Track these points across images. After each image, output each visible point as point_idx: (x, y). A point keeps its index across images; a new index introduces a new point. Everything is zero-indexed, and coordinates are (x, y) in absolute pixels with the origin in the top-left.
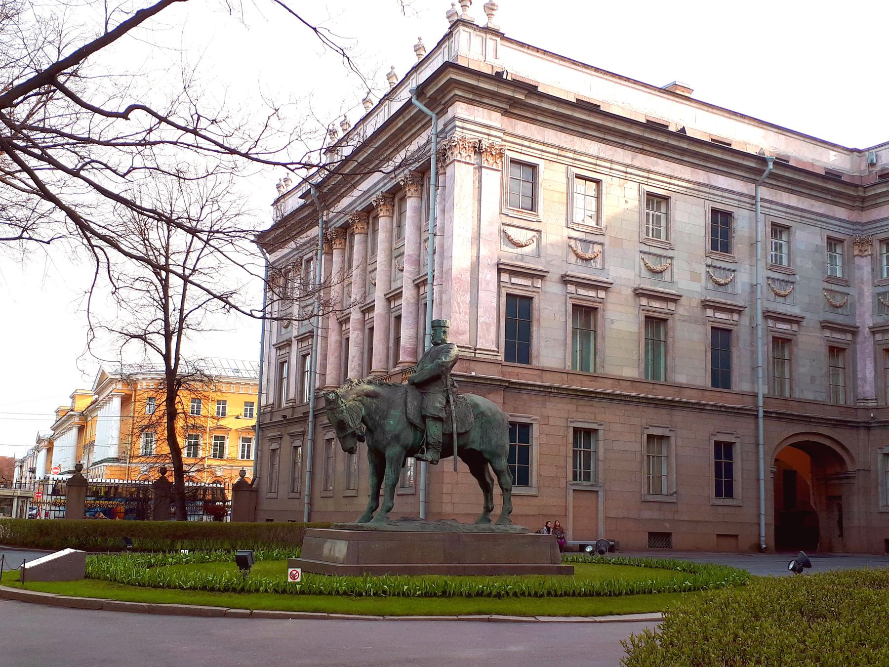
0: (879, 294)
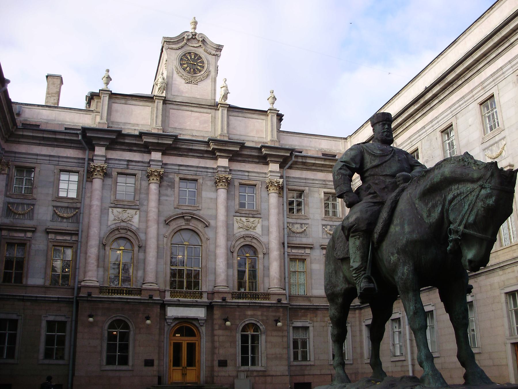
0: (9, 203)
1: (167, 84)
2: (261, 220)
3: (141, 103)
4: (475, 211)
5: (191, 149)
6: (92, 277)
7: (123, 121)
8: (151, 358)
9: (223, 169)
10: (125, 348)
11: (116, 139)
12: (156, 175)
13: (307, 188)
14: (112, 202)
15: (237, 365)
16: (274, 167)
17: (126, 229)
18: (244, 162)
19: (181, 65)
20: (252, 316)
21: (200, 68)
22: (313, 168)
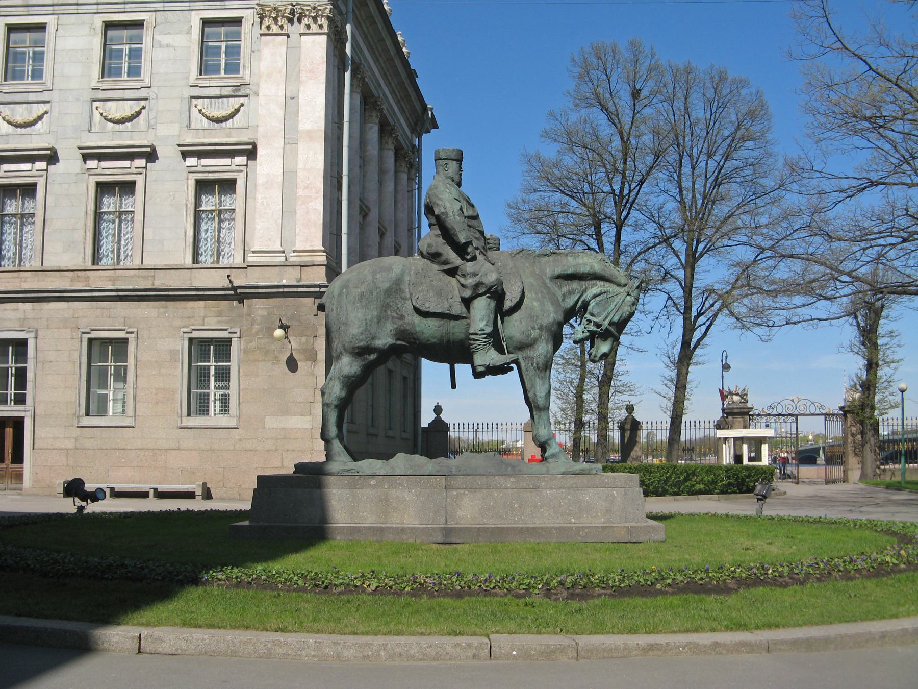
4: (619, 313)
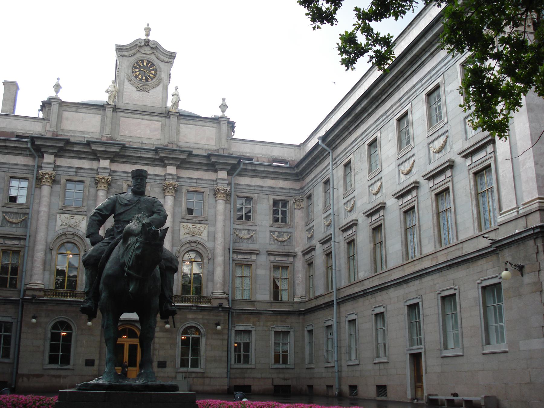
1: (118, 92)
2: (207, 226)
3: (92, 111)
5: (140, 157)
6: (38, 280)
7: (73, 129)
8: (92, 358)
9: (170, 177)
10: (67, 349)
11: (64, 147)
12: (103, 183)
13: (256, 195)
14: (60, 208)
15: (177, 367)
16: (223, 175)
17: (73, 234)
18: (193, 169)
19: (133, 72)
20: (193, 319)
21: (152, 76)
22: (263, 175)
